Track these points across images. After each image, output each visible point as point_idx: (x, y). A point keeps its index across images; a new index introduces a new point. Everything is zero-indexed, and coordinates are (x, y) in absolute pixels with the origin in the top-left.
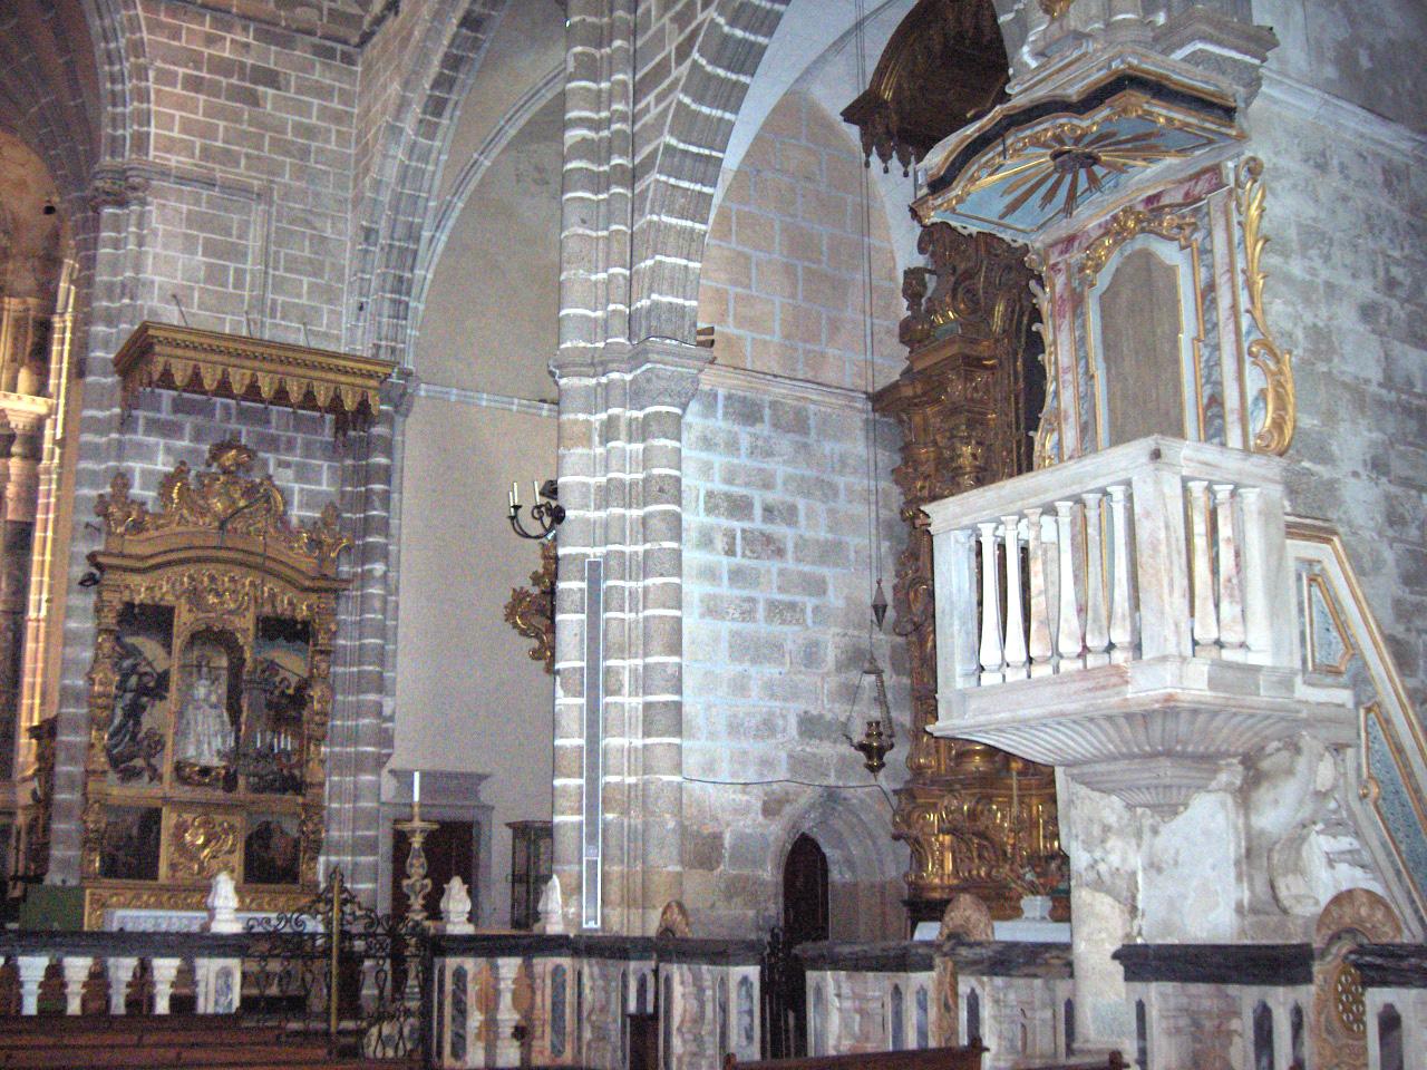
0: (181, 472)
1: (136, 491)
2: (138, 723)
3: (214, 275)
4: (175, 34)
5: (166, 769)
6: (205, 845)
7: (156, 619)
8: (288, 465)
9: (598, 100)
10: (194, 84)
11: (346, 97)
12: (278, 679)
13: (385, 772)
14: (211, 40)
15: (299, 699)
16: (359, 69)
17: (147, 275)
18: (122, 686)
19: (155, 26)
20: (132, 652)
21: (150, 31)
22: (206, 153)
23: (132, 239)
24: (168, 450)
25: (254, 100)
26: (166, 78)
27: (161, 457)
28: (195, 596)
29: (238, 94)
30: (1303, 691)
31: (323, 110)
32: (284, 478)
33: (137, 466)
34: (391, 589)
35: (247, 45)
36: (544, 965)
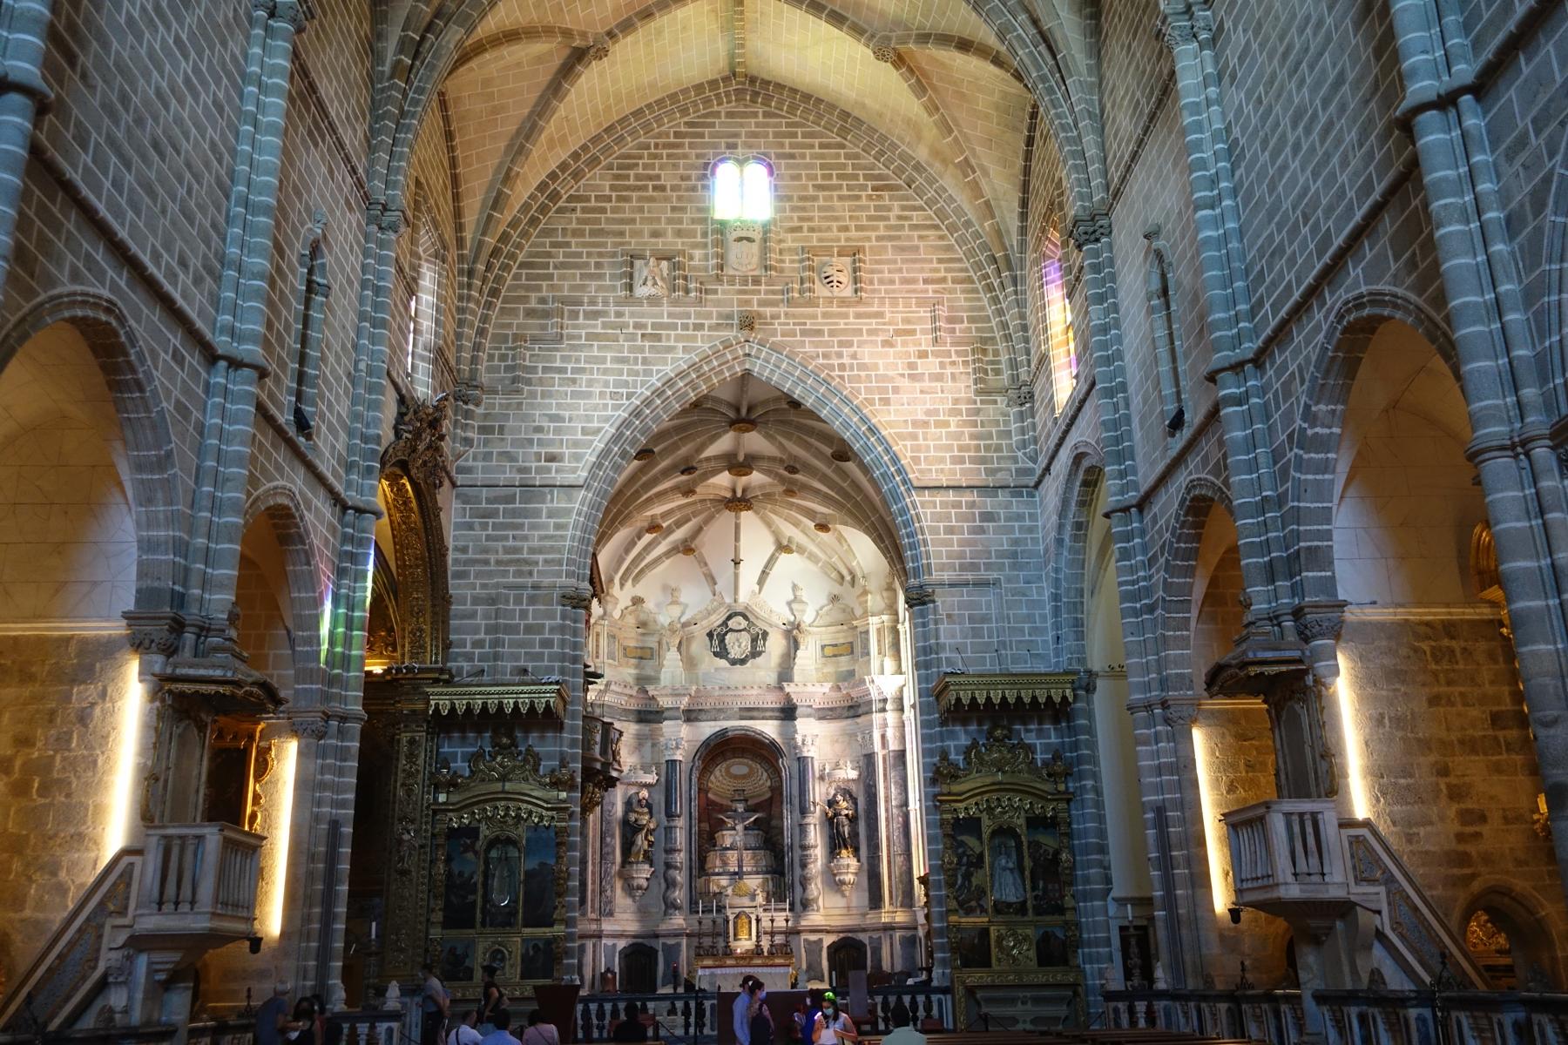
0: (975, 744)
1: (952, 757)
2: (970, 882)
3: (976, 633)
5: (989, 902)
6: (1014, 947)
7: (972, 826)
8: (1031, 731)
13: (1109, 898)
16: (1037, 499)
17: (942, 640)
18: (960, 863)
20: (962, 844)
23: (931, 622)
24: (966, 732)
27: (963, 736)
28: (990, 810)
30: (1355, 889)
31: (1021, 528)
32: (1030, 739)
33: (952, 744)
34: (1098, 791)
36: (1160, 1005)
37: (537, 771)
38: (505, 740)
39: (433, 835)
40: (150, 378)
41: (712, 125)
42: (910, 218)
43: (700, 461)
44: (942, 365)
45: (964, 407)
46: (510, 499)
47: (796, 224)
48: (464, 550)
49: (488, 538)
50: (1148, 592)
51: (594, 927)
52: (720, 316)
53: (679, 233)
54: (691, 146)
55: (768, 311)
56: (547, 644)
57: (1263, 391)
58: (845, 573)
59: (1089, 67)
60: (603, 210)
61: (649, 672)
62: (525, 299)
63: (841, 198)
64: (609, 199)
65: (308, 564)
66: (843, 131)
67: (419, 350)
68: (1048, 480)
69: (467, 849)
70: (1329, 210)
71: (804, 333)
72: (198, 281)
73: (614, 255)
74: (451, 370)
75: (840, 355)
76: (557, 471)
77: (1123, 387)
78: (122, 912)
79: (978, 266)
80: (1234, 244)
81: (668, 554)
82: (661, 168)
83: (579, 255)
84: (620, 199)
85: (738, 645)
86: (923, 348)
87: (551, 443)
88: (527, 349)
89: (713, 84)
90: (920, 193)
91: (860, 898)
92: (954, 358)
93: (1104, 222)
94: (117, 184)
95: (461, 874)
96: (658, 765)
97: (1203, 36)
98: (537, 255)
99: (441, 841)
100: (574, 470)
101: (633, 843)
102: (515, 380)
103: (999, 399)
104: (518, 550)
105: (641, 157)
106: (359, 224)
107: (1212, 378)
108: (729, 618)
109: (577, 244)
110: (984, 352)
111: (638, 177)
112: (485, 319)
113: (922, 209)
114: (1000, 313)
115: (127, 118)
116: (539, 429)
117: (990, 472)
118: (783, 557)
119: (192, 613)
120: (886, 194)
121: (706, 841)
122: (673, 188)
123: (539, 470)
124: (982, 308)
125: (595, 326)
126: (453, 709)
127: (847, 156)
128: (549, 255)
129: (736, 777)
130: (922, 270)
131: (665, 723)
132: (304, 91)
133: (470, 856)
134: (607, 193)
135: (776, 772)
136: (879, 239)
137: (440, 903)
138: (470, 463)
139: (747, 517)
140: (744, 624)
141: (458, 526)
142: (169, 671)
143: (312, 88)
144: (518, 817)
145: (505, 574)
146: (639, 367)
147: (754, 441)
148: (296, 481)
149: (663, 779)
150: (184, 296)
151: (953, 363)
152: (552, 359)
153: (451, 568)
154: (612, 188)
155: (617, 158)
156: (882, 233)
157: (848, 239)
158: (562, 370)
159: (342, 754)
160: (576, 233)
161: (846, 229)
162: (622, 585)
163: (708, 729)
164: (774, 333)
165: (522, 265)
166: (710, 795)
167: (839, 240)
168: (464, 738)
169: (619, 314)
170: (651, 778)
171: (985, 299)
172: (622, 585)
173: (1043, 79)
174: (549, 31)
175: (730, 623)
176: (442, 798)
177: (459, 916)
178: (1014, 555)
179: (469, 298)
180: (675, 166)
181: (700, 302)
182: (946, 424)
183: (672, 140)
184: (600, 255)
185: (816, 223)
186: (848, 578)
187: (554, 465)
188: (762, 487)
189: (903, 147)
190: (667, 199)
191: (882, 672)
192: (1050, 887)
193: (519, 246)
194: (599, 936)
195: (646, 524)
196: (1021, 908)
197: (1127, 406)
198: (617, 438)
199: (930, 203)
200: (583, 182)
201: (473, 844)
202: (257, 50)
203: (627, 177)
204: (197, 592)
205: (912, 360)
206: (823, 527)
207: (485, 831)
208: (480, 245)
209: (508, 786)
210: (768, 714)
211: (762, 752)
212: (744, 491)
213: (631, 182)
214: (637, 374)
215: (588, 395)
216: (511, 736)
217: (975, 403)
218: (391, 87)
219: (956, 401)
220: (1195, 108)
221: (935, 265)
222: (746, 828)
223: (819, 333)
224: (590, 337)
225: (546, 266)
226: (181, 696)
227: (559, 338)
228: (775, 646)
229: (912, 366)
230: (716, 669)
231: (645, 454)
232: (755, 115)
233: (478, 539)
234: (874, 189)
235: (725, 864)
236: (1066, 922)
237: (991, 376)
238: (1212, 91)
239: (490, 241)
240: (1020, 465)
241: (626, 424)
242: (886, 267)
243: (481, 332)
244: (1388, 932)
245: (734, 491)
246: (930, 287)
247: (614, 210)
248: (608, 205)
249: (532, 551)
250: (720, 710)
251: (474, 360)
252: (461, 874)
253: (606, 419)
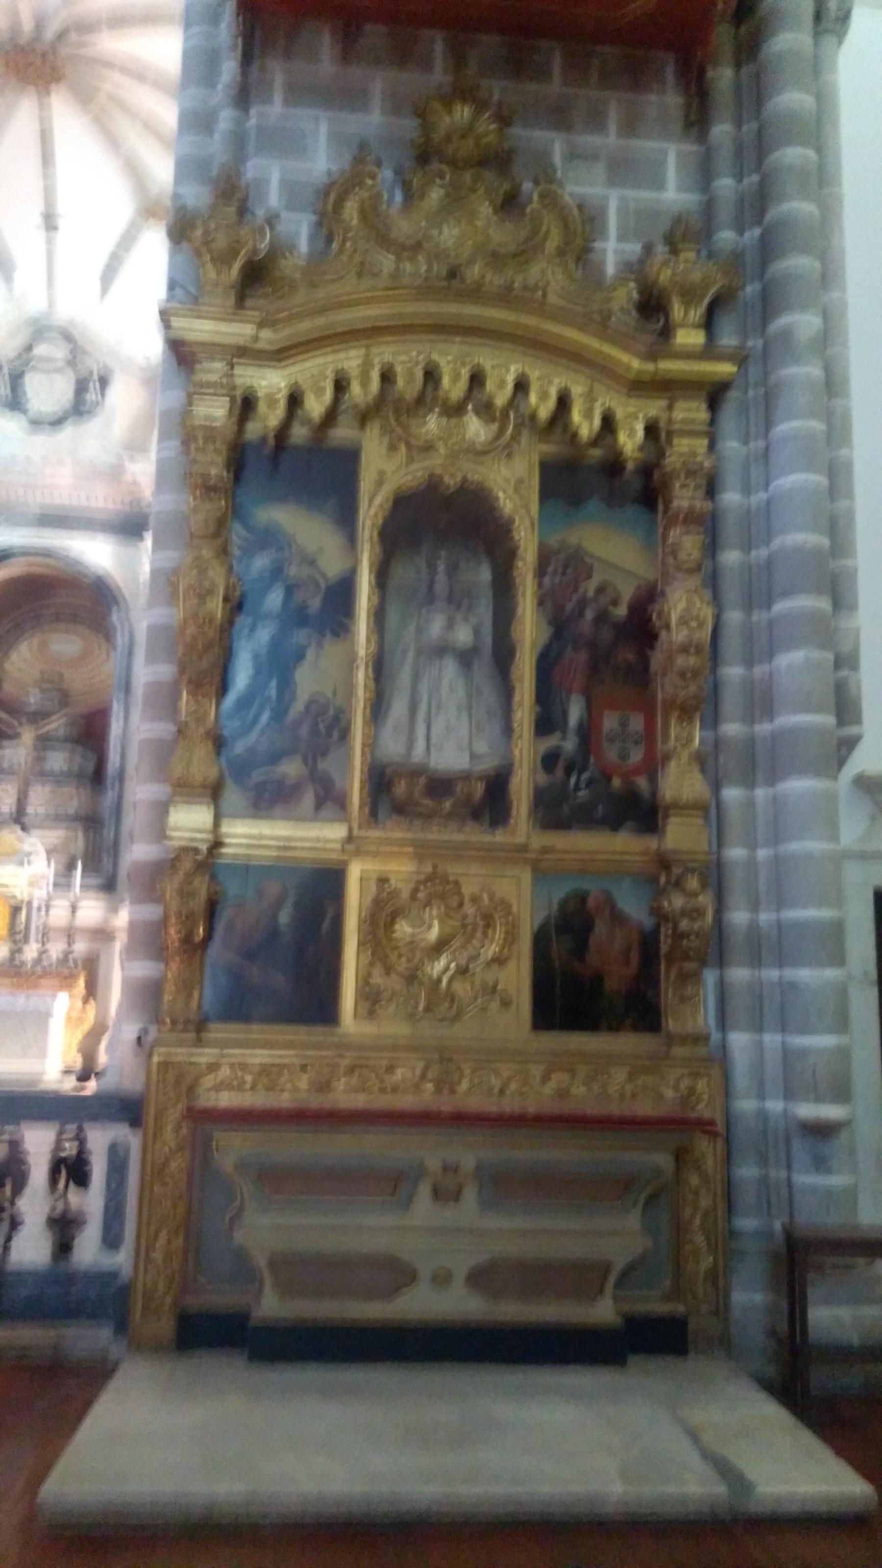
2: (286, 685)
8: (591, 157)
12: (590, 587)
192: (610, 722)
236: (664, 862)
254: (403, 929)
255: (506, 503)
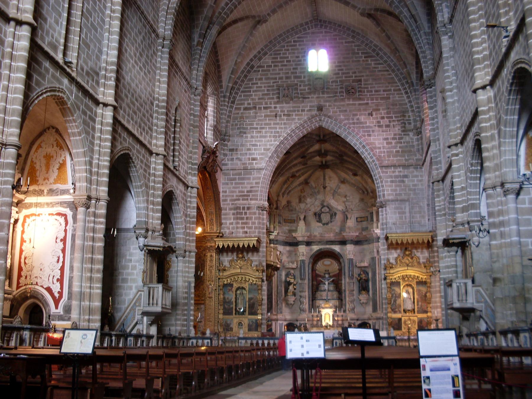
0: (399, 255)
3: (401, 218)
4: (387, 172)
9: (439, 202)
10: (392, 182)
11: (421, 176)
14: (394, 172)
15: (426, 296)
18: (392, 296)
19: (383, 172)
21: (382, 173)
22: (396, 195)
24: (396, 252)
25: (403, 182)
26: (387, 182)
29: (400, 181)
31: (417, 180)
35: (401, 171)
37: (251, 266)
38: (240, 256)
39: (219, 286)
40: (137, 164)
41: (307, 37)
42: (378, 68)
43: (308, 154)
44: (390, 122)
45: (397, 137)
46: (240, 174)
47: (337, 72)
48: (226, 192)
49: (234, 188)
50: (444, 209)
51: (275, 317)
52: (311, 106)
53: (296, 77)
54: (299, 45)
55: (327, 104)
56: (254, 223)
57: (461, 153)
58: (364, 190)
59: (429, 28)
60: (269, 71)
61: (294, 228)
62: (244, 104)
63: (353, 61)
64: (271, 66)
65: (178, 206)
66: (353, 37)
67: (209, 127)
68: (426, 163)
69: (230, 290)
70: (472, 103)
71: (340, 111)
72: (147, 133)
73: (273, 86)
74: (219, 131)
75: (353, 119)
76: (256, 164)
77: (438, 139)
78: (140, 306)
79: (403, 85)
80: (457, 105)
81: (299, 185)
82: (289, 53)
83: (261, 87)
84: (275, 66)
85: (325, 218)
86: (383, 115)
87: (254, 154)
88: (244, 121)
89: (307, 23)
90: (382, 58)
91: (369, 309)
92: (394, 119)
93: (433, 81)
94: (128, 115)
95: (228, 298)
96: (297, 262)
97: (449, 34)
98: (247, 88)
99: (221, 287)
100: (261, 164)
101: (288, 289)
102: (240, 132)
103: (410, 133)
104: (243, 192)
105: (282, 50)
106: (189, 96)
107: (449, 147)
108: (322, 208)
109: (261, 83)
110: (404, 116)
111: (281, 58)
112: (230, 112)
113: (382, 64)
114: (410, 102)
115: (130, 96)
116: (249, 150)
117: (406, 160)
118: (343, 186)
119: (150, 227)
120: (369, 59)
121: (315, 289)
122: (293, 61)
123: (249, 164)
124: (404, 100)
125: (267, 112)
126: (223, 246)
127: (355, 46)
128: (250, 88)
129: (326, 265)
130: (382, 87)
131: (300, 246)
132: (172, 63)
133: (231, 292)
134: (270, 64)
135: (340, 263)
136: (367, 76)
137: (222, 307)
138: (227, 162)
139: (329, 172)
140: (328, 210)
141: (223, 184)
142: (146, 244)
143: (174, 61)
144: (245, 280)
145: (239, 200)
146: (283, 126)
147: (327, 146)
148: (173, 182)
149: (299, 266)
150: (145, 138)
151: (394, 121)
152: (252, 124)
153: (221, 198)
154: (272, 62)
155: (274, 51)
156: (368, 73)
157: (355, 77)
158: (257, 128)
159: (190, 262)
160: (261, 79)
161: (355, 73)
162: (283, 197)
163: (315, 248)
164: (330, 112)
165: (243, 92)
166: (317, 272)
167: (352, 77)
168: (227, 255)
169: (275, 108)
170: (294, 266)
171: (405, 96)
172: (283, 197)
173: (413, 30)
174: (247, 17)
175: (323, 210)
176: (221, 274)
177: (227, 312)
178: (415, 190)
179: (225, 105)
180: (294, 53)
181: (303, 102)
182: (391, 143)
183: (293, 43)
184: (269, 87)
185: (344, 71)
186: (366, 193)
187: (254, 162)
188: (332, 160)
189: (375, 42)
190: (291, 65)
191: (378, 228)
193: (241, 85)
194: (277, 320)
195: (290, 175)
196: (413, 311)
197: (440, 146)
198: (276, 151)
199: (386, 62)
200: (261, 61)
201: (231, 289)
202: (159, 59)
203: (277, 58)
204: (151, 221)
205: (379, 120)
206: (355, 175)
207: (235, 285)
208: (228, 86)
209: (242, 271)
210: (337, 243)
211: (335, 256)
212: (326, 162)
213: (279, 59)
214: (282, 128)
215: (265, 137)
216: (242, 253)
217: (401, 135)
218: (198, 49)
219: (395, 135)
220: (447, 58)
221: (387, 85)
222: (329, 284)
223: (346, 111)
224: (266, 116)
225: (250, 91)
226: (149, 250)
227: (256, 117)
228: (339, 217)
229: (379, 122)
230: (318, 227)
231: (288, 153)
232: (322, 32)
233: (230, 188)
234: (365, 57)
235: (321, 296)
237: (407, 125)
238: (452, 53)
239: (231, 85)
240: (417, 157)
241: (279, 146)
242: (369, 86)
243: (229, 116)
244: (484, 317)
245: (322, 162)
246: (385, 93)
247: (273, 70)
248: (271, 69)
249: (248, 192)
250: (319, 242)
251: (226, 127)
252: (228, 298)
253: (271, 145)
254: (407, 323)
255: (413, 285)
